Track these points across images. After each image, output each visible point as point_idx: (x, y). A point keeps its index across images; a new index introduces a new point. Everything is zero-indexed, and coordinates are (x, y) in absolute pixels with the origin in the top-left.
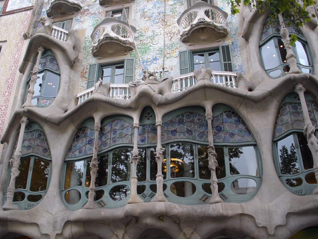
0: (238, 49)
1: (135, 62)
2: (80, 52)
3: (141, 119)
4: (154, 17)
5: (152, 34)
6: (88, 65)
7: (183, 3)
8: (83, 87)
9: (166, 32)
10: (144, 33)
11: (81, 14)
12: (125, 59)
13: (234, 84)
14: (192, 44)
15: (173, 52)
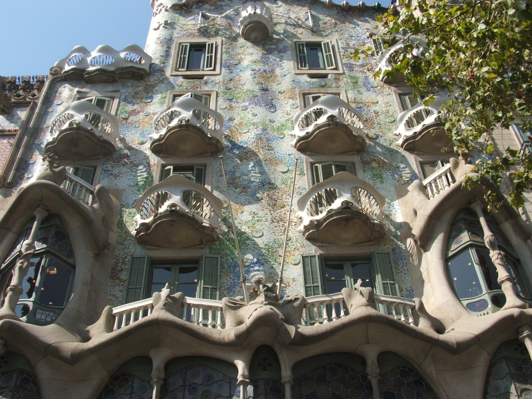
0: (404, 262)
1: (221, 264)
2: (112, 231)
3: (251, 367)
4: (253, 188)
5: (250, 218)
6: (126, 257)
7: (305, 172)
8: (114, 298)
9: (277, 218)
10: (235, 215)
11: (114, 162)
12: (202, 256)
13: (411, 320)
14: (324, 244)
15: (290, 254)
